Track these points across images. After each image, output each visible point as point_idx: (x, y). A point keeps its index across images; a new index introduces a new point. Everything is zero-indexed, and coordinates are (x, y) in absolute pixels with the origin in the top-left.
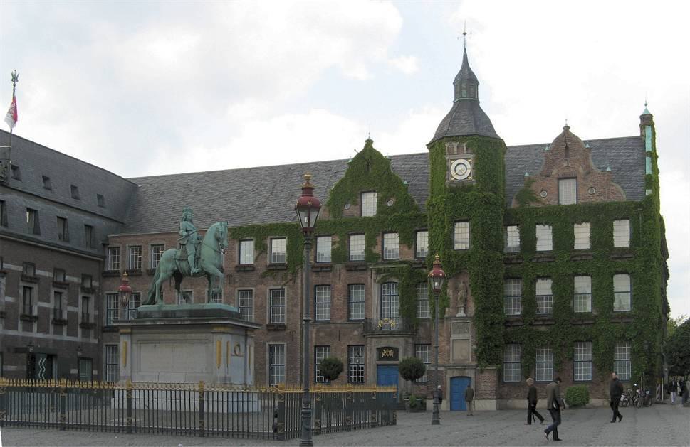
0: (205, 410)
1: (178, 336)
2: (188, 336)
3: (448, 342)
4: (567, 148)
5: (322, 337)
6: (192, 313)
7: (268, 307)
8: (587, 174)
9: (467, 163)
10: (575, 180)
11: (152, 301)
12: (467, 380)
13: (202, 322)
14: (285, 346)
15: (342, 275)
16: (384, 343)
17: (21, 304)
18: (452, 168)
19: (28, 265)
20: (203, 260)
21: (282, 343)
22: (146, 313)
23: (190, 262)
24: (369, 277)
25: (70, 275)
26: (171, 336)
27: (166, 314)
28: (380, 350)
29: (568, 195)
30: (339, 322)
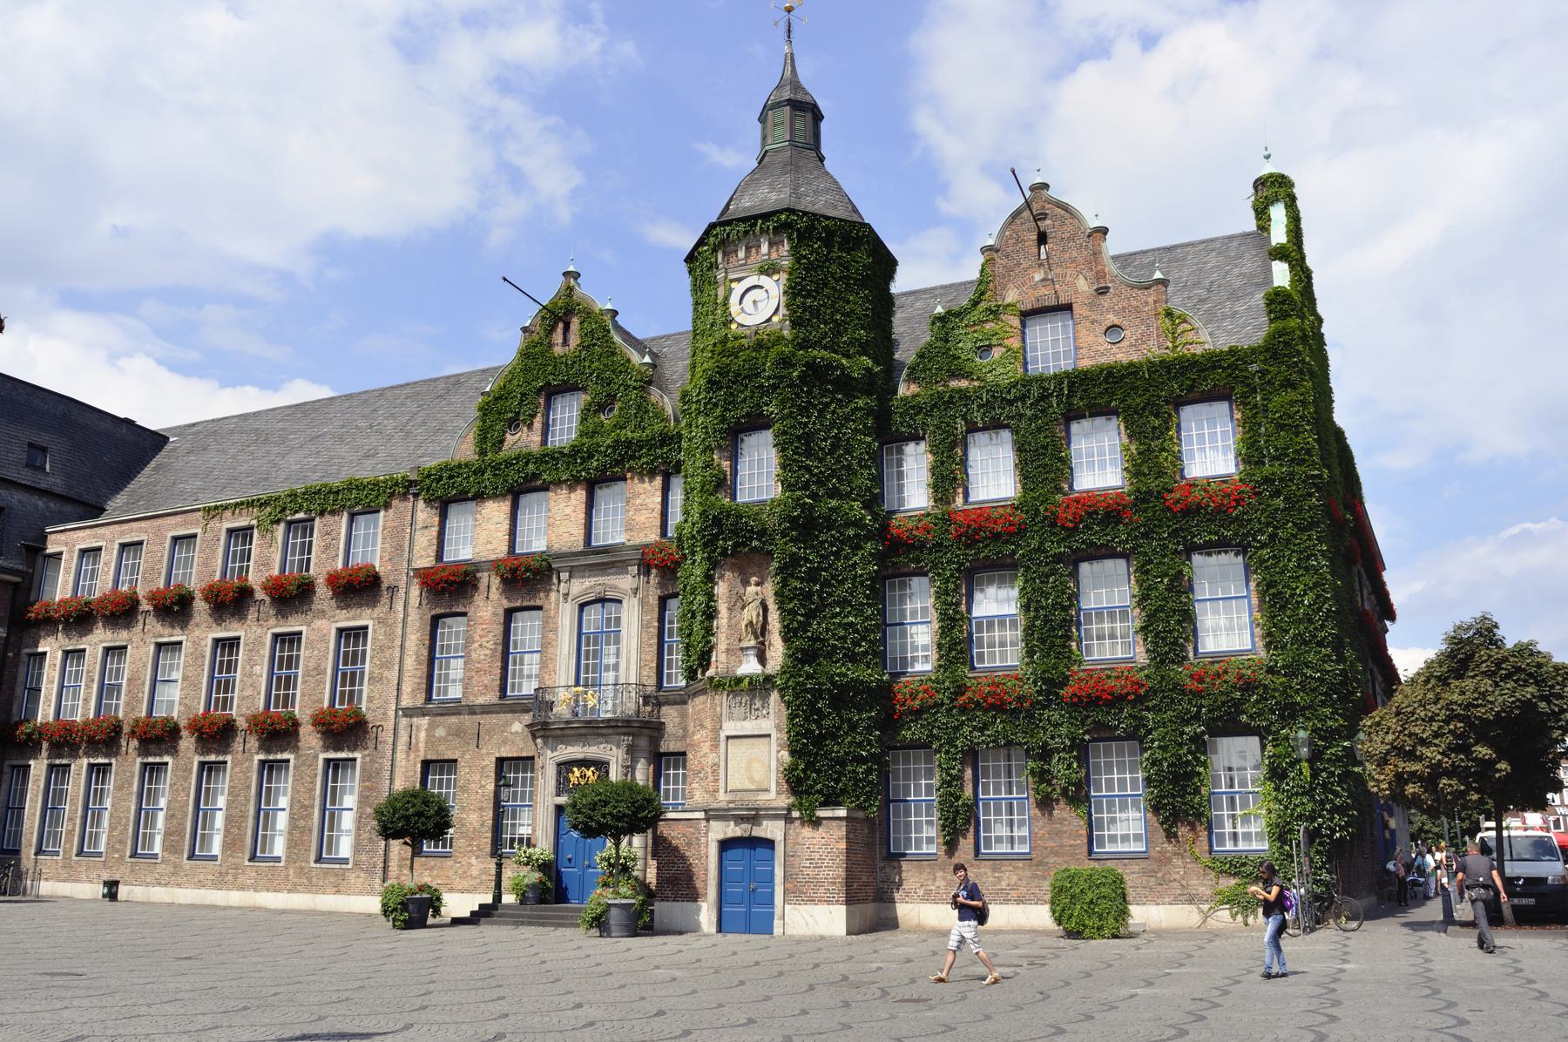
5: (439, 739)
7: (329, 671)
10: (1067, 315)
15: (493, 589)
28: (565, 767)
29: (1053, 350)
30: (481, 700)
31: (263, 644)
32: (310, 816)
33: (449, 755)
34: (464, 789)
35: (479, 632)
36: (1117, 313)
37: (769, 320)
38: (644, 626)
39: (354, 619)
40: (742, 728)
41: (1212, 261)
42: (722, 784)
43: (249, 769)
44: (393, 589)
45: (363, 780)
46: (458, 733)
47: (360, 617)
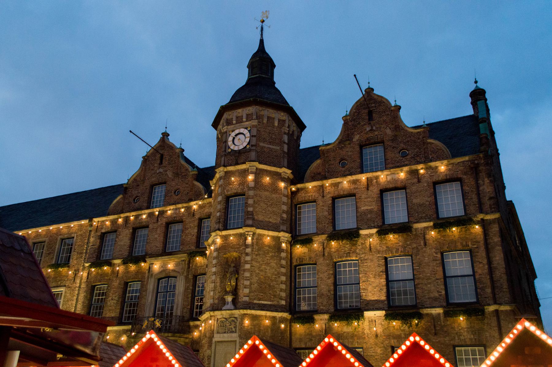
3: (210, 346)
9: (246, 132)
18: (230, 139)
36: (405, 143)
37: (245, 147)
40: (223, 337)
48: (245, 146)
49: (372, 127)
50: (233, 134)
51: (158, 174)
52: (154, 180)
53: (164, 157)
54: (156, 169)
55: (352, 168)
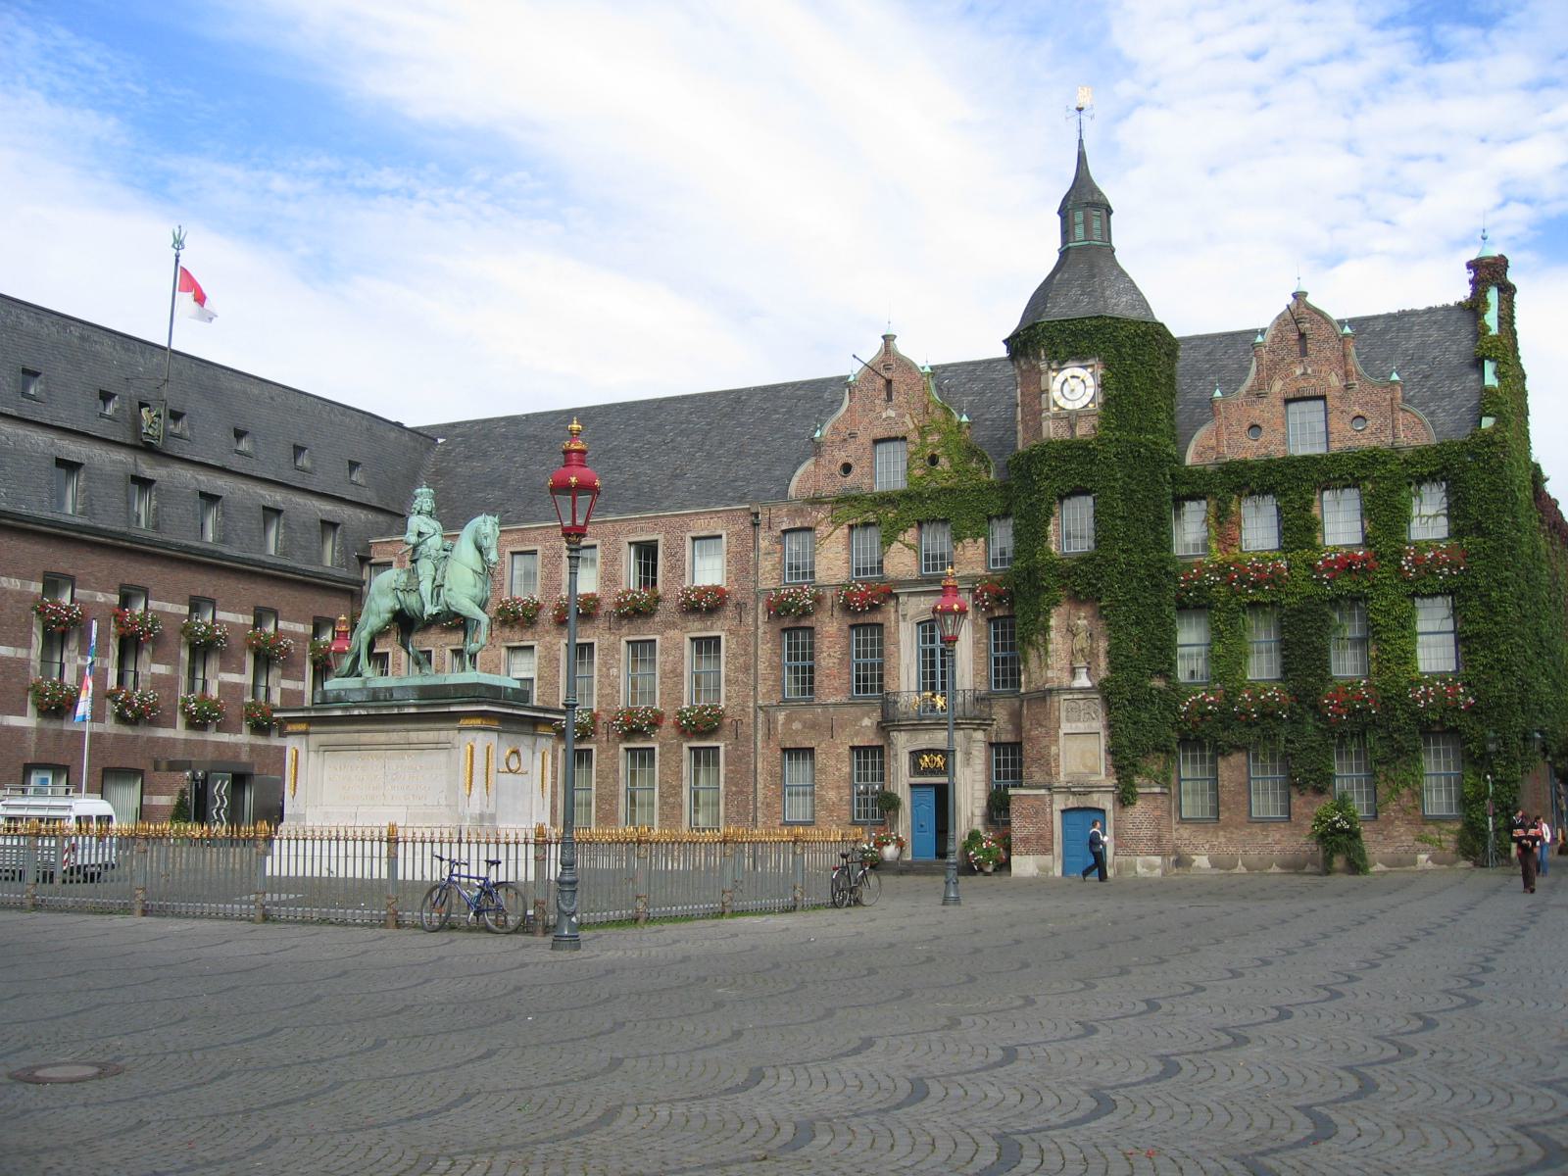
0: (400, 877)
1: (395, 737)
2: (414, 736)
4: (1302, 336)
5: (796, 731)
6: (426, 693)
8: (1347, 387)
10: (1322, 403)
11: (354, 671)
12: (1096, 816)
13: (438, 708)
14: (722, 750)
16: (924, 740)
17: (184, 678)
19: (196, 605)
20: (449, 590)
21: (715, 744)
22: (339, 695)
23: (423, 595)
24: (892, 610)
25: (288, 619)
26: (381, 737)
27: (375, 695)
28: (916, 755)
30: (832, 700)
31: (618, 651)
32: (679, 794)
33: (807, 744)
34: (823, 771)
35: (826, 643)
36: (1361, 406)
37: (1086, 406)
38: (976, 643)
39: (705, 630)
41: (1434, 334)
42: (1061, 769)
43: (616, 756)
44: (740, 606)
45: (727, 764)
46: (813, 726)
47: (712, 628)
48: (1085, 403)
49: (1305, 369)
50: (1061, 377)
51: (885, 420)
52: (880, 433)
53: (894, 384)
54: (878, 409)
55: (1271, 442)
